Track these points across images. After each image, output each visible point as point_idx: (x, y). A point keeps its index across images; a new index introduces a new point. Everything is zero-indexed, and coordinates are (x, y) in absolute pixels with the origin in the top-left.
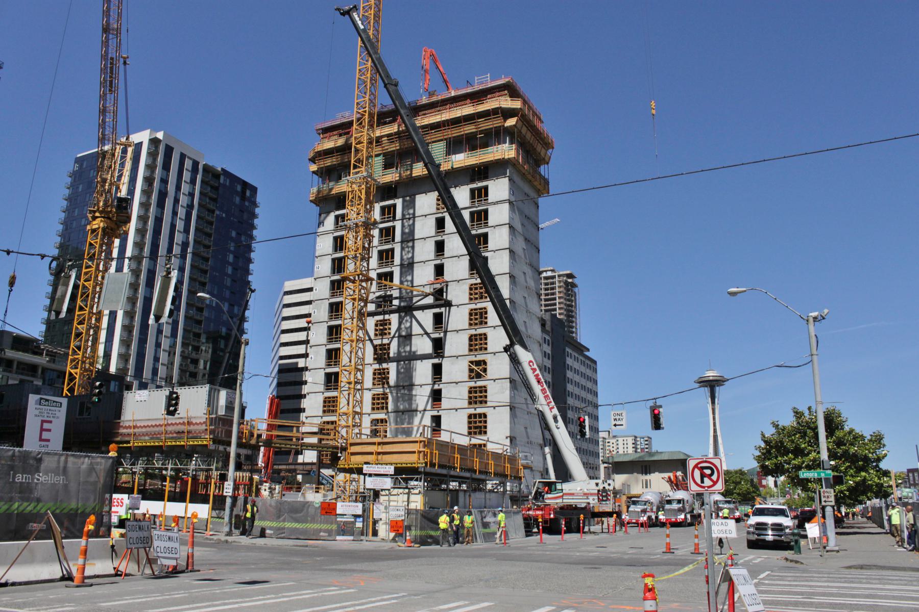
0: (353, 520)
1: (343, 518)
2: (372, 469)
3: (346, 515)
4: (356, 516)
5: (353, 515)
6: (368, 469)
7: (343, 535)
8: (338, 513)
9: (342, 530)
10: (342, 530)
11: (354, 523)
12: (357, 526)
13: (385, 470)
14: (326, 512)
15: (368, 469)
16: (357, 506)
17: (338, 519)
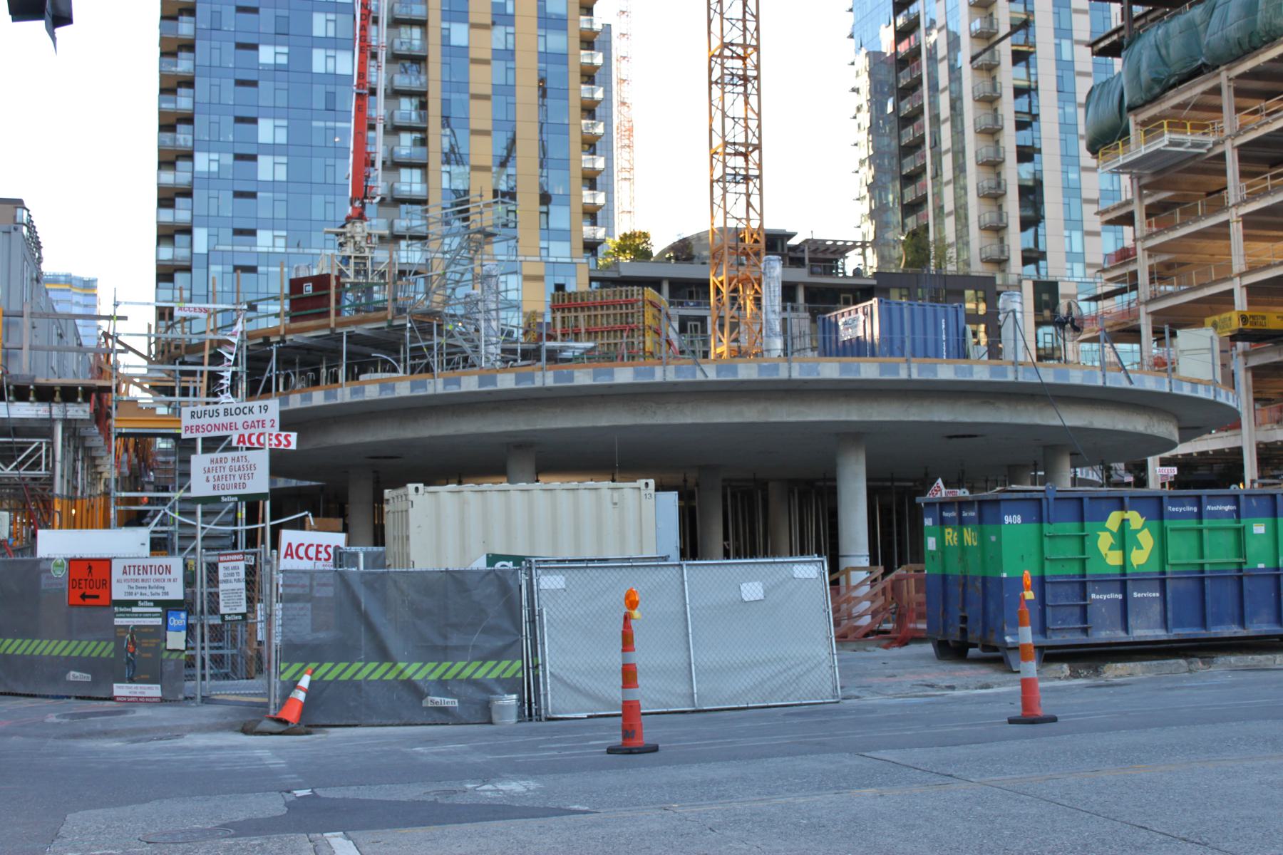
0: (158, 621)
1: (131, 615)
2: (206, 421)
3: (134, 603)
4: (169, 607)
5: (157, 603)
6: (196, 422)
7: (131, 680)
8: (115, 597)
9: (129, 660)
10: (129, 660)
11: (159, 633)
12: (169, 646)
13: (250, 418)
14: (83, 597)
15: (196, 422)
16: (168, 569)
17: (118, 621)
